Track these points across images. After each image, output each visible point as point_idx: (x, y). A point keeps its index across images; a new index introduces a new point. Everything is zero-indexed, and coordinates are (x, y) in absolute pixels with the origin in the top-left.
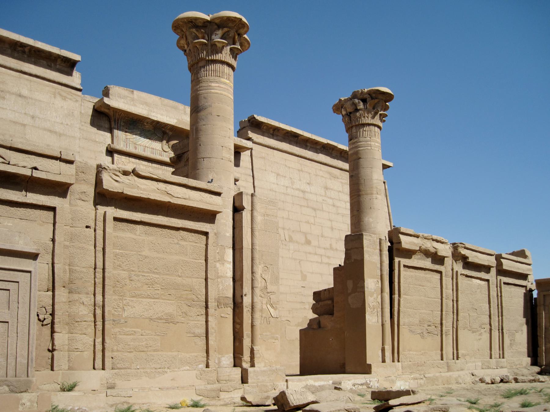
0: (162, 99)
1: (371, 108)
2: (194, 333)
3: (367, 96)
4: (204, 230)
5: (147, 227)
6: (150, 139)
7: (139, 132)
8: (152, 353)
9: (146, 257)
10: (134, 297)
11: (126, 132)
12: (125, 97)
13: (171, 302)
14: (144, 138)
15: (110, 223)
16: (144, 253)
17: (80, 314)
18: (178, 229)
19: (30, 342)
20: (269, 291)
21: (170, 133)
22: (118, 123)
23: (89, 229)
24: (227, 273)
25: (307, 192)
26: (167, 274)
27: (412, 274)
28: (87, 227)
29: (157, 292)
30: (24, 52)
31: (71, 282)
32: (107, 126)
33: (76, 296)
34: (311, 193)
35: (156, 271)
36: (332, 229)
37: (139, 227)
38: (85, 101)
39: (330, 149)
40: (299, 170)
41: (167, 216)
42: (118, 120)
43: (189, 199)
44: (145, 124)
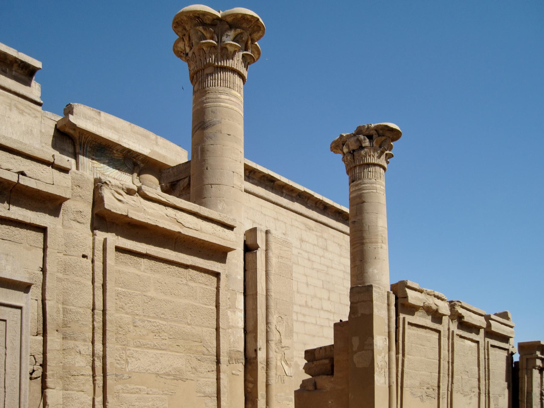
0: (133, 125)
1: (378, 146)
2: (204, 393)
3: (374, 132)
4: (216, 270)
5: (153, 262)
6: (119, 170)
7: (107, 161)
9: (152, 299)
10: (138, 347)
11: (93, 159)
12: (91, 119)
13: (180, 354)
14: (113, 168)
15: (111, 253)
16: (149, 294)
17: (77, 365)
18: (186, 267)
19: (22, 400)
20: (283, 345)
22: (84, 148)
23: (85, 259)
24: (238, 323)
26: (175, 321)
27: (414, 332)
28: (84, 256)
29: (164, 342)
31: (65, 325)
32: (71, 150)
33: (71, 343)
35: (163, 316)
36: (307, 284)
37: (145, 262)
38: (45, 118)
39: (306, 197)
40: (275, 219)
41: (175, 249)
42: (84, 145)
44: (115, 152)
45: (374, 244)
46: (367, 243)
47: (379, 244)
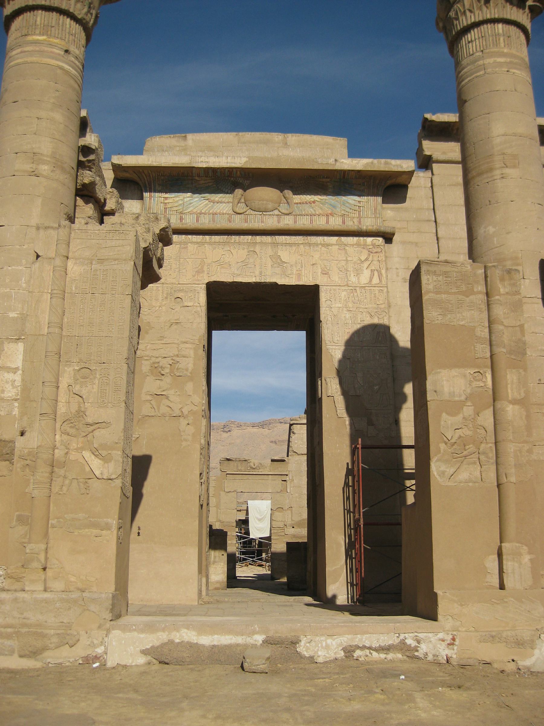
0: (241, 134)
12: (171, 148)
44: (197, 178)
45: (485, 176)
46: (473, 178)
47: (497, 173)
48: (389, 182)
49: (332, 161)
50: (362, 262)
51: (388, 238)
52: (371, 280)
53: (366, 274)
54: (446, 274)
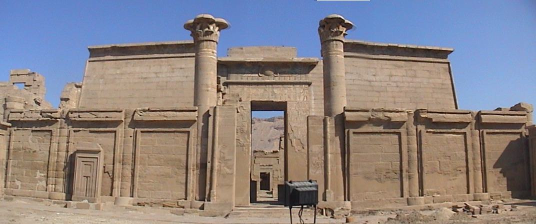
2: (180, 182)
8: (157, 191)
21: (263, 65)
25: (373, 81)
28: (131, 137)
30: (183, 47)
34: (376, 81)
43: (176, 116)
48: (310, 64)
49: (291, 59)
50: (301, 93)
51: (309, 84)
52: (304, 99)
53: (302, 97)
54: (315, 119)
